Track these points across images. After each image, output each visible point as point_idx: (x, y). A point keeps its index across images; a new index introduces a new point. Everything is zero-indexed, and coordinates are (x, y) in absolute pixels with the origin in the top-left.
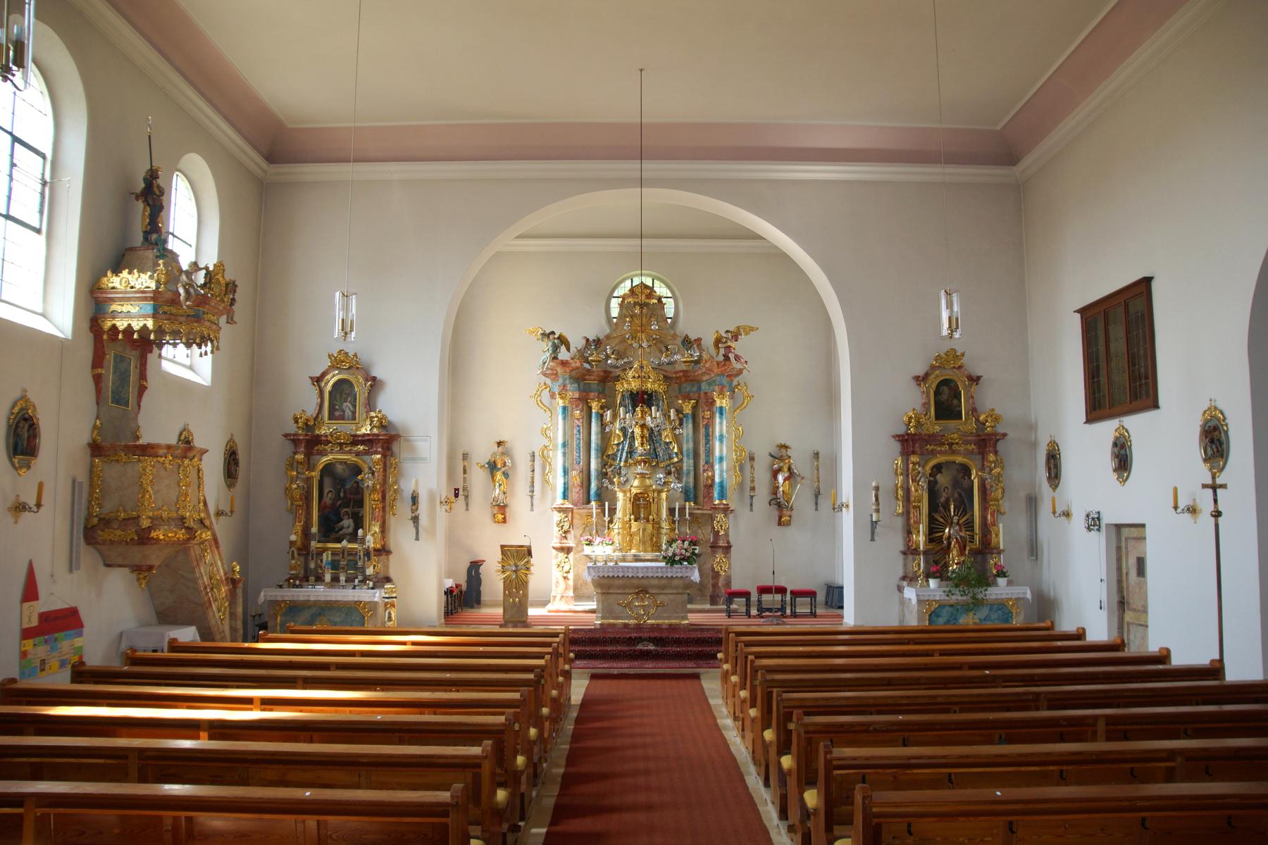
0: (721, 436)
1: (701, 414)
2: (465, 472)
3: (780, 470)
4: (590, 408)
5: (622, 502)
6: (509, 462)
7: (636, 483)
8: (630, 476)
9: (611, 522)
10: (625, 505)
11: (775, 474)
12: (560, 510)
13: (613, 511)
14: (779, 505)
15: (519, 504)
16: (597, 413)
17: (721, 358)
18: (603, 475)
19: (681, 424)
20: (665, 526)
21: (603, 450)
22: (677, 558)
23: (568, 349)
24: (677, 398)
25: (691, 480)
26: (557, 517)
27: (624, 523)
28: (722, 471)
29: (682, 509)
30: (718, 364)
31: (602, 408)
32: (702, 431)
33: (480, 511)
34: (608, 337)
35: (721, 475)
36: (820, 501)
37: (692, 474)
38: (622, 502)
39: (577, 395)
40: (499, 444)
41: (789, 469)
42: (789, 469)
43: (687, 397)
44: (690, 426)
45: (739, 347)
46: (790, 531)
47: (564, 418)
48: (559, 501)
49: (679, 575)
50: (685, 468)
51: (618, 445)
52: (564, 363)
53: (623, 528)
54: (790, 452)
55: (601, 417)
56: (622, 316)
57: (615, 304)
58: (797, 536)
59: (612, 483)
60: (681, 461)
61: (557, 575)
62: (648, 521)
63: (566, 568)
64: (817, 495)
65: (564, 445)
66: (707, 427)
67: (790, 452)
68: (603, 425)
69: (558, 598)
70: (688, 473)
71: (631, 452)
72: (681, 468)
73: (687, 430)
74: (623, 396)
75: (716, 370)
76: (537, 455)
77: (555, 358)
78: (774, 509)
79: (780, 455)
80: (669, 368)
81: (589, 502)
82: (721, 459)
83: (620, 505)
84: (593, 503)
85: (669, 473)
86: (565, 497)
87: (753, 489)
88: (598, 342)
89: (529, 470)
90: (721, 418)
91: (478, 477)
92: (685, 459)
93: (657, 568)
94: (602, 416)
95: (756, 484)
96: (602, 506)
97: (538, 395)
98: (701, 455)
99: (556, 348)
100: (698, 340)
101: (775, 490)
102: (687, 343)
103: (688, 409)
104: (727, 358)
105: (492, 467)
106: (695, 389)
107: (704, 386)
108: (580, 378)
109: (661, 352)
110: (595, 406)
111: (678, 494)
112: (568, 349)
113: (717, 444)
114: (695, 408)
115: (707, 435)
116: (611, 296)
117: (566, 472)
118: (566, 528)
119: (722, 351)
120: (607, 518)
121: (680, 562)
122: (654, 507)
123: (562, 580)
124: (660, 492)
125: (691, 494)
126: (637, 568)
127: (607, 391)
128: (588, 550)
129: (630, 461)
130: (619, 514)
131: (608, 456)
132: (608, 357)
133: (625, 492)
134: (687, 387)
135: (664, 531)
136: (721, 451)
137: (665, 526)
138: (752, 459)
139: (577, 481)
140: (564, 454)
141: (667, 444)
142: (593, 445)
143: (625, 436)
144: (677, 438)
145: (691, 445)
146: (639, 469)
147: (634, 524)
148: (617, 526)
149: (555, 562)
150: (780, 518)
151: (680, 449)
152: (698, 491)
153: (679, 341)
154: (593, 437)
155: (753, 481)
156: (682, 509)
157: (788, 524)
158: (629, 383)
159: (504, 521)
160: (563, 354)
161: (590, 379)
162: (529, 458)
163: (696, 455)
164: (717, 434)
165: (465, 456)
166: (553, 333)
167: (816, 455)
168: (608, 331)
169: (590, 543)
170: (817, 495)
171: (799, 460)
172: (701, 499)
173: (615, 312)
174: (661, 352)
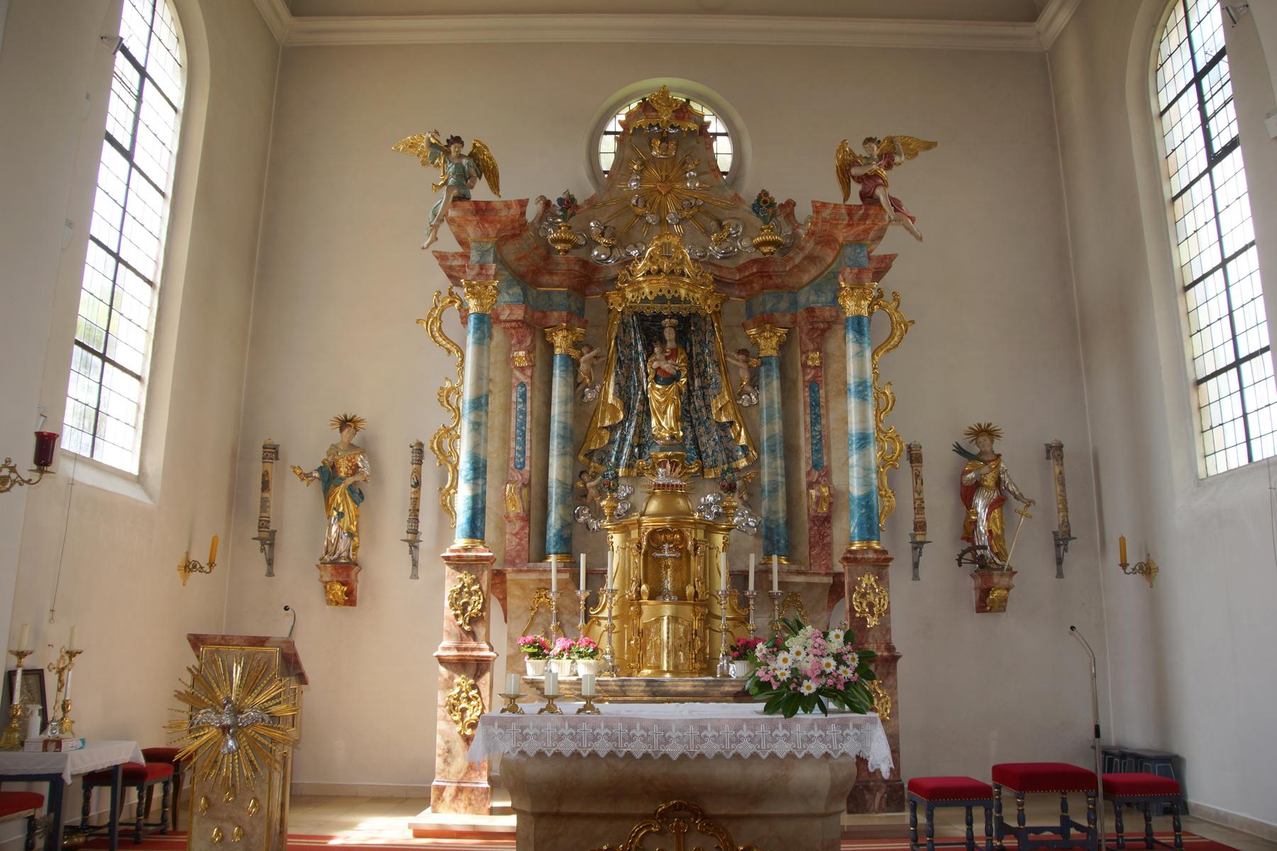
0: (862, 384)
1: (799, 358)
2: (265, 486)
3: (977, 486)
4: (551, 347)
5: (618, 555)
6: (359, 460)
7: (654, 506)
8: (640, 497)
9: (592, 602)
10: (625, 560)
11: (967, 494)
12: (458, 563)
13: (597, 576)
14: (983, 566)
15: (385, 562)
16: (567, 357)
17: (855, 200)
18: (576, 495)
19: (754, 383)
20: (722, 609)
21: (577, 443)
22: (809, 687)
23: (495, 186)
24: (745, 327)
25: (781, 506)
26: (452, 581)
27: (624, 604)
28: (866, 469)
29: (764, 573)
30: (851, 210)
31: (576, 345)
32: (803, 395)
33: (299, 578)
34: (591, 203)
35: (865, 481)
36: (1067, 557)
37: (781, 493)
38: (618, 555)
39: (519, 314)
40: (346, 423)
41: (998, 482)
42: (998, 482)
43: (765, 321)
44: (776, 384)
45: (899, 182)
46: (1006, 624)
47: (480, 342)
48: (460, 542)
49: (818, 749)
50: (766, 479)
51: (612, 429)
52: (482, 211)
53: (623, 617)
54: (998, 447)
55: (572, 365)
56: (619, 162)
57: (608, 145)
58: (1021, 632)
59: (598, 514)
60: (755, 465)
61: (446, 729)
62: (681, 597)
63: (472, 715)
64: (1062, 540)
65: (479, 403)
66: (813, 385)
67: (998, 447)
68: (577, 387)
69: (448, 795)
70: (774, 490)
71: (643, 442)
72: (757, 481)
73: (771, 392)
74: (624, 326)
75: (841, 235)
76: (426, 449)
77: (462, 198)
78: (970, 568)
79: (978, 446)
80: (726, 263)
81: (543, 556)
82: (863, 440)
83: (614, 562)
84: (552, 559)
85: (731, 488)
86: (475, 530)
87: (920, 526)
88: (568, 204)
89: (409, 482)
90: (859, 342)
91: (297, 502)
92: (765, 459)
93: (738, 725)
94: (576, 364)
95: (929, 517)
96: (571, 565)
97: (435, 319)
98: (802, 446)
99: (464, 179)
100: (790, 204)
101: (968, 530)
102: (764, 204)
103: (769, 346)
104: (869, 198)
105: (328, 477)
106: (784, 305)
107: (806, 297)
108: (527, 277)
109: (708, 233)
110: (560, 341)
111: (750, 541)
112: (495, 186)
113: (853, 403)
114: (783, 346)
115: (815, 405)
116: (599, 131)
117: (478, 470)
118: (473, 610)
119: (856, 188)
120: (582, 593)
121: (808, 703)
122: (696, 566)
123: (459, 745)
124: (710, 529)
125: (774, 539)
126: (664, 725)
127: (589, 314)
128: (533, 669)
129: (641, 463)
130: (613, 582)
131: (590, 455)
132: (591, 244)
133: (625, 530)
134: (767, 302)
135: (721, 624)
136: (863, 419)
137: (722, 609)
138: (914, 456)
139: (515, 508)
140: (476, 426)
141: (723, 427)
142: (555, 427)
143: (628, 409)
144: (745, 415)
145: (778, 427)
146: (662, 476)
147: (648, 607)
148: (607, 610)
149: (442, 698)
150: (984, 593)
151: (754, 440)
152: (796, 532)
153: (745, 211)
154: (556, 409)
155: (919, 509)
156: (764, 573)
157: (1001, 606)
158: (637, 288)
159: (350, 599)
160: (480, 191)
161: (544, 278)
162: (408, 456)
163: (790, 451)
164: (852, 380)
165: (272, 452)
166: (457, 140)
167: (1054, 451)
168: (591, 191)
169: (540, 652)
170: (1062, 540)
171: (1017, 460)
172: (804, 550)
173: (607, 162)
174: (708, 233)
